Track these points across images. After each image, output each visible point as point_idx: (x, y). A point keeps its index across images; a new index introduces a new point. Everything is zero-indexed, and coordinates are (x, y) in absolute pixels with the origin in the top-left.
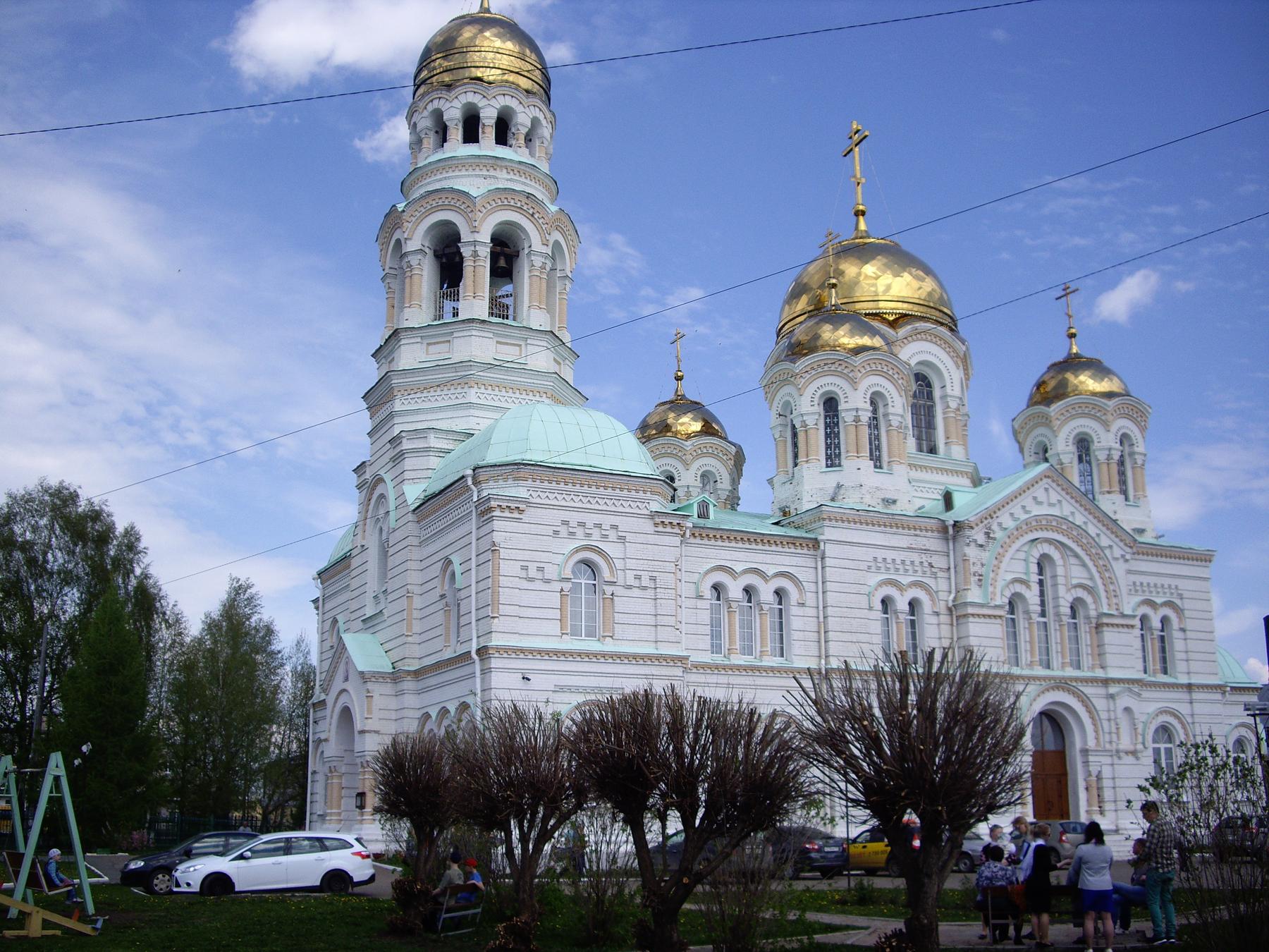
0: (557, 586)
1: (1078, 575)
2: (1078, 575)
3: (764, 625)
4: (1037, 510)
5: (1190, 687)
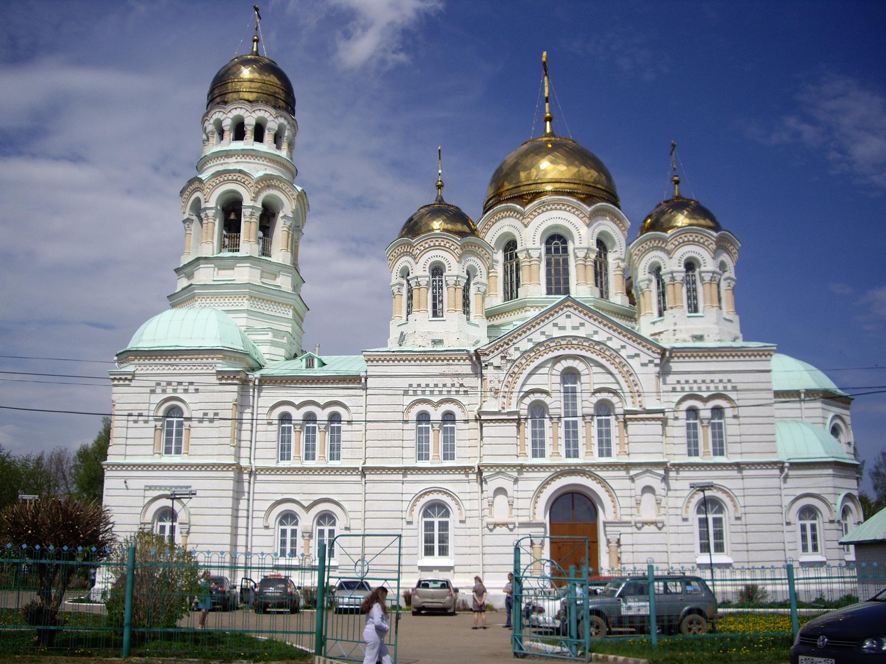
0: (152, 424)
1: (600, 379)
2: (600, 379)
3: (322, 440)
4: (557, 333)
5: (739, 466)
